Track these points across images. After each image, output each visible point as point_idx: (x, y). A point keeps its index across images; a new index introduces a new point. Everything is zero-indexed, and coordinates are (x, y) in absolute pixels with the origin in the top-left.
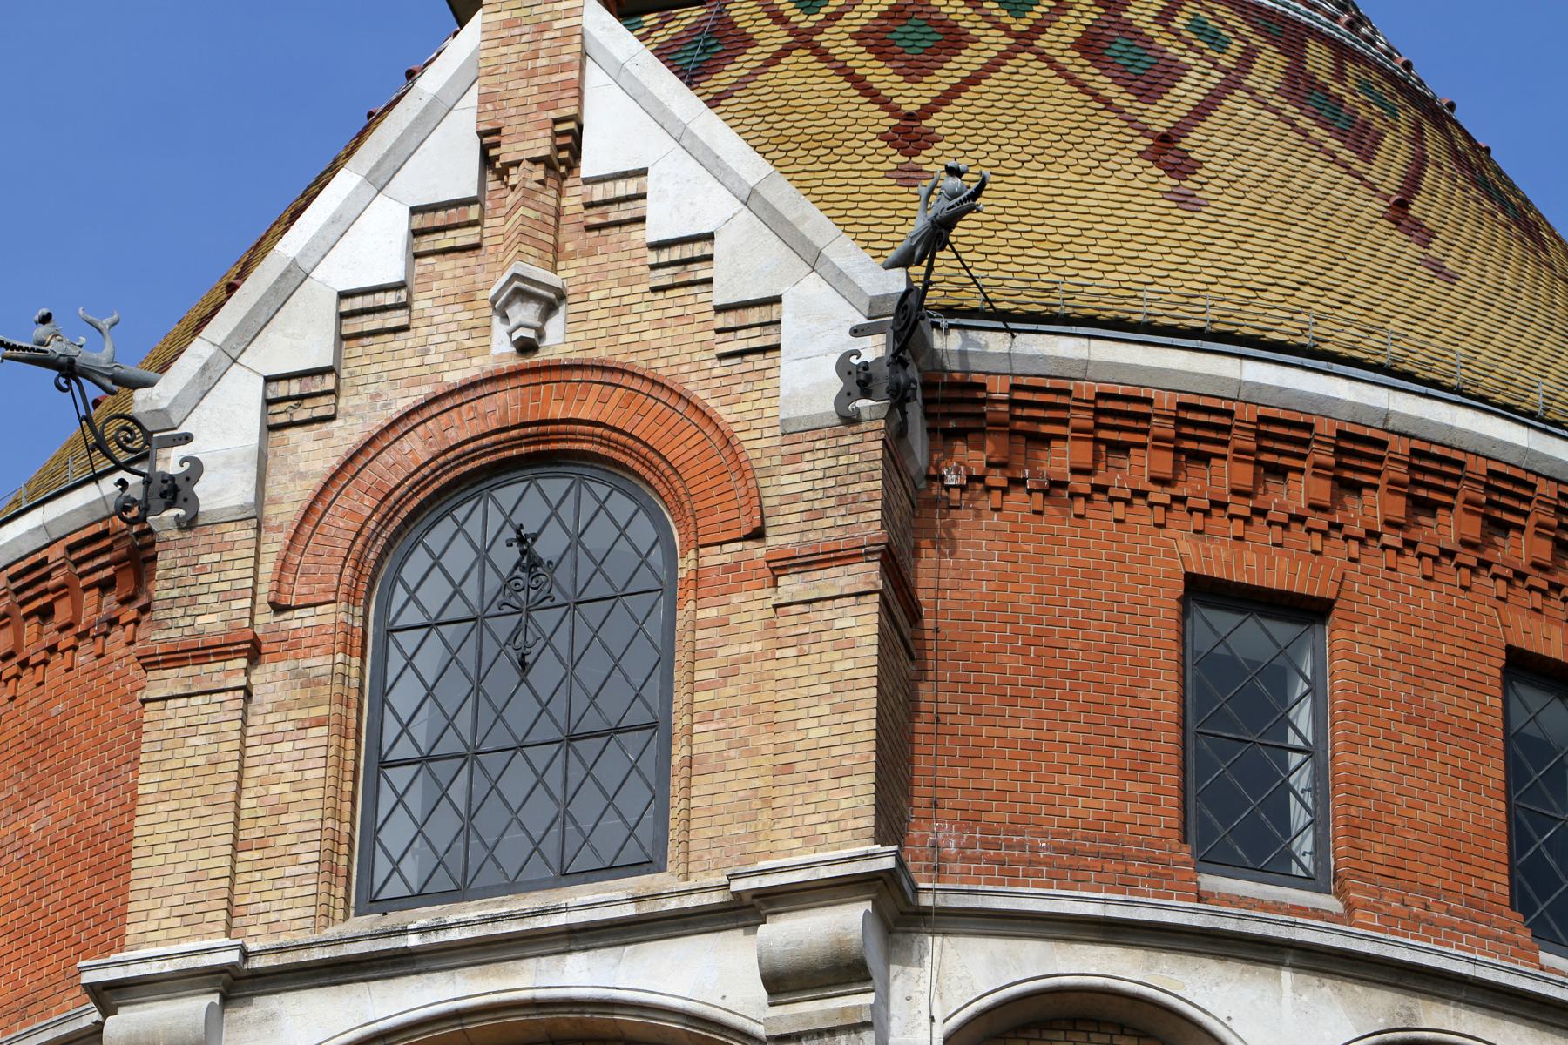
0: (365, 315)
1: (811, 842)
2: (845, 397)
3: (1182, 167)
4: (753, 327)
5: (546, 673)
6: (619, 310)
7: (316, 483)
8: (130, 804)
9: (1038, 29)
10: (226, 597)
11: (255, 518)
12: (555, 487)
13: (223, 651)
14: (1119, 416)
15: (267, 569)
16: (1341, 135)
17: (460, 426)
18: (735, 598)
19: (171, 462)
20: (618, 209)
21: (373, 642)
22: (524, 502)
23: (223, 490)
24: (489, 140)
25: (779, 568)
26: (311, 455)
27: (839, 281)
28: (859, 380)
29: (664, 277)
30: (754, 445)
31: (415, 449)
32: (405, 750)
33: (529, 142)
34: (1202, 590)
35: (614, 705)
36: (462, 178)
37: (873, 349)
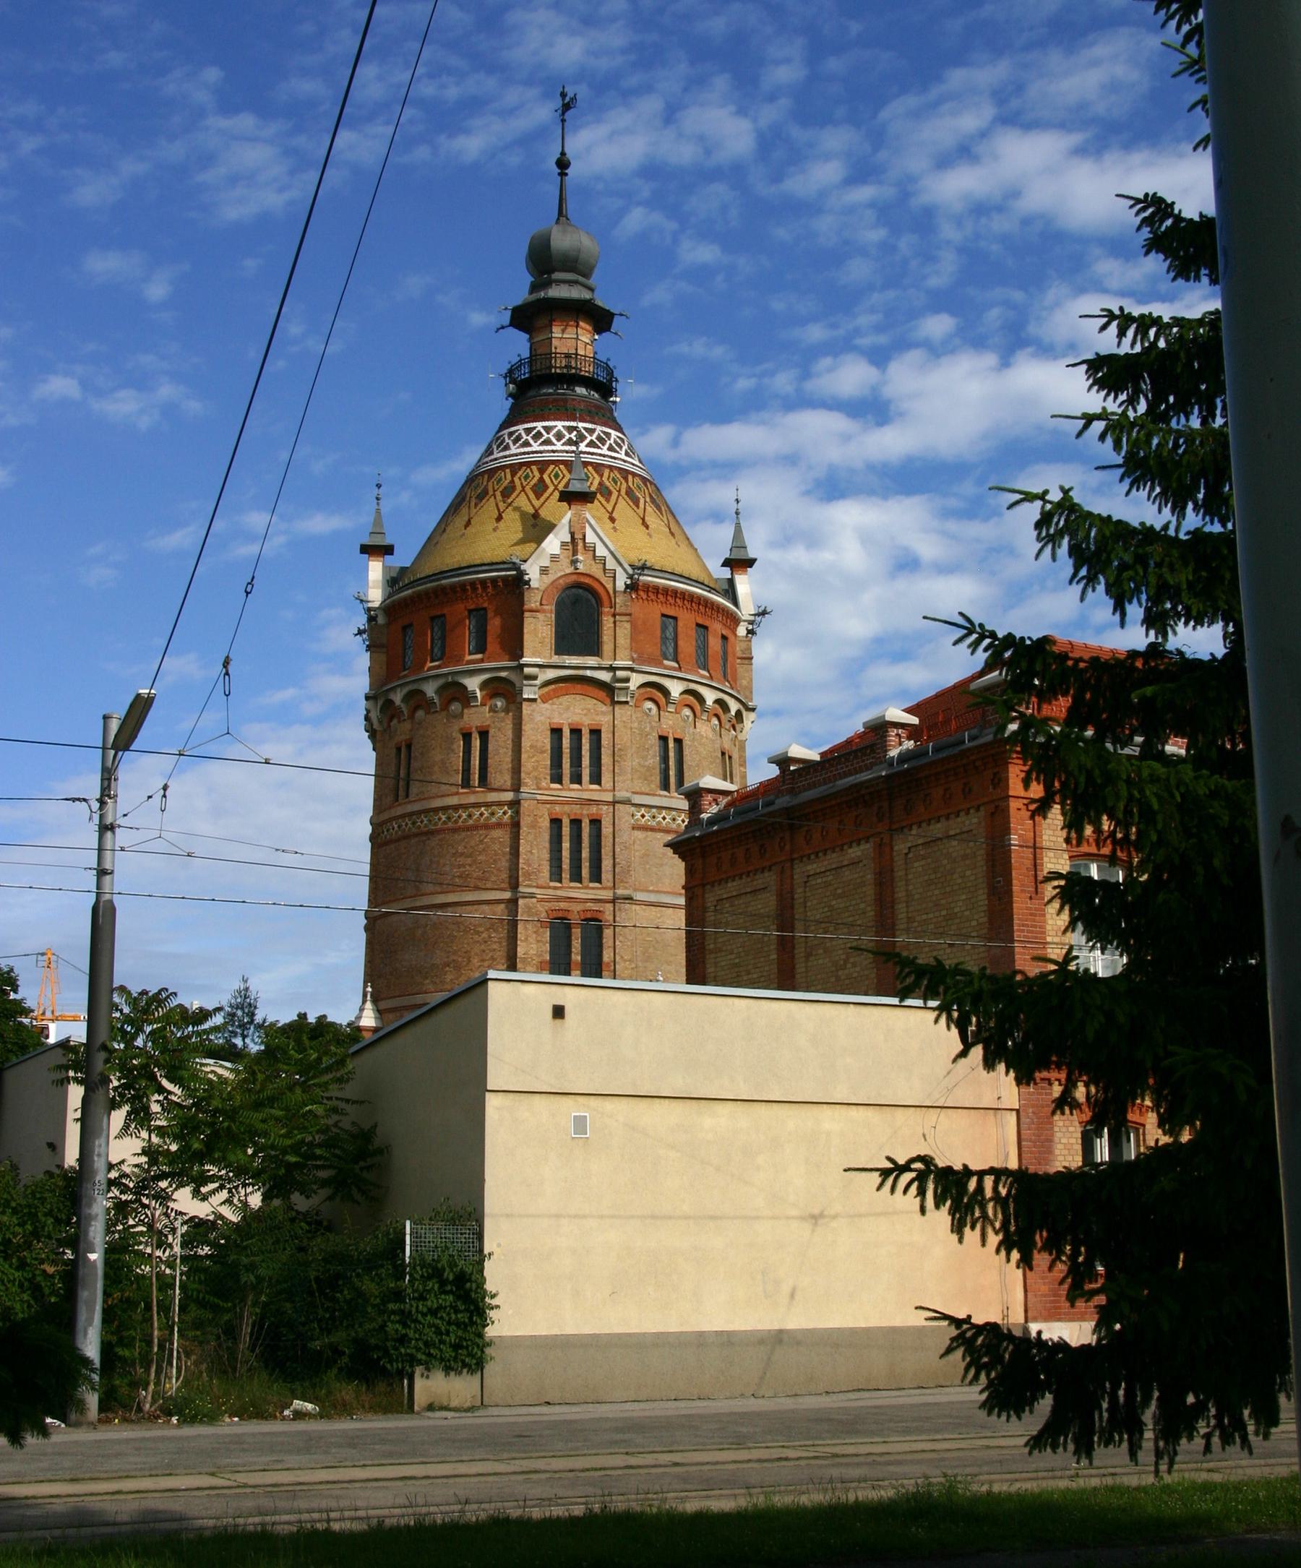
0: (554, 558)
14: (657, 590)
19: (526, 578)
23: (534, 584)
26: (548, 580)
27: (625, 570)
37: (629, 582)
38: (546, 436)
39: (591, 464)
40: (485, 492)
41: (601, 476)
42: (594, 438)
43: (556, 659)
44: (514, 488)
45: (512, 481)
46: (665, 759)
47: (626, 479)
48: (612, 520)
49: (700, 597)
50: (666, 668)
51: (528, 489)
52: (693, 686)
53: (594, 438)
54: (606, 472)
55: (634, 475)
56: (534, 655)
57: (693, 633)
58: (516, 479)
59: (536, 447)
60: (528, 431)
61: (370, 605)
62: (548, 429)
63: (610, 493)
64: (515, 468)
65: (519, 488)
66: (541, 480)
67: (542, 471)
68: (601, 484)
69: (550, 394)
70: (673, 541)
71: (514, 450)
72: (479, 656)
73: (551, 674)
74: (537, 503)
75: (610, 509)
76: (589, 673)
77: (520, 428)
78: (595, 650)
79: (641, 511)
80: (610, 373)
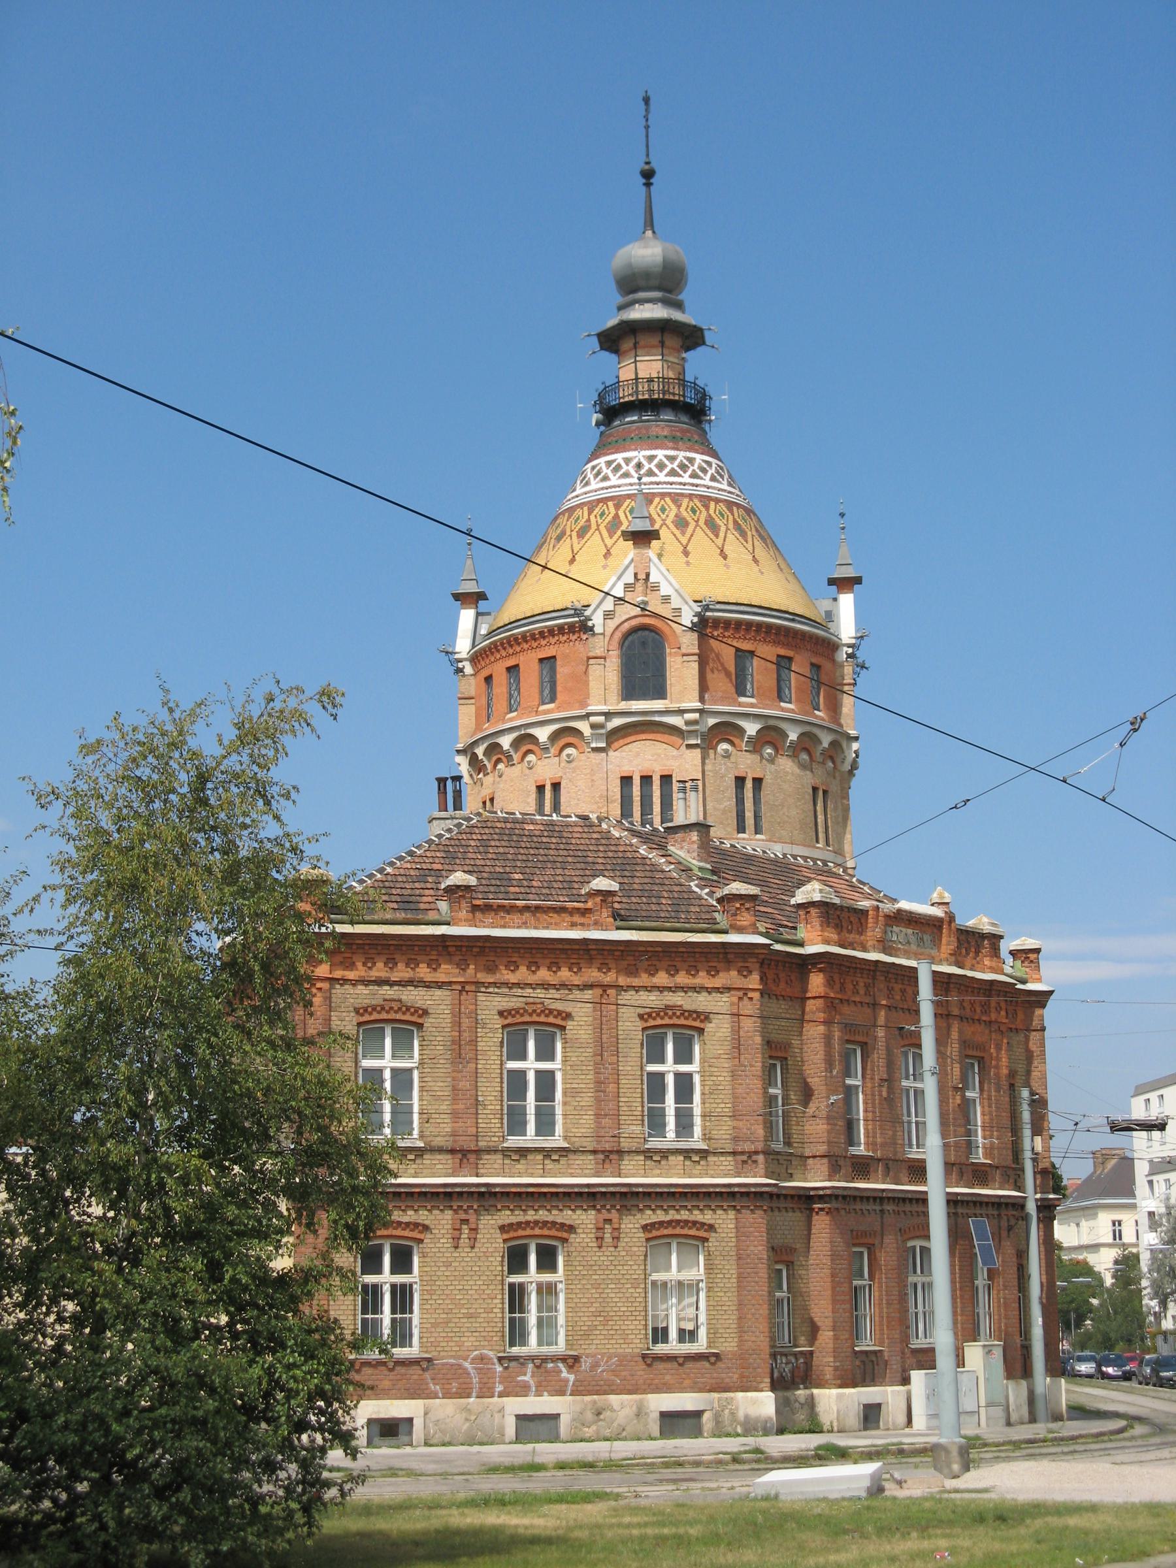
1: (690, 701)
11: (603, 634)
17: (634, 622)
19: (590, 624)
20: (656, 588)
24: (636, 574)
25: (684, 655)
26: (612, 624)
31: (627, 626)
33: (642, 576)
37: (696, 620)
38: (625, 468)
39: (670, 494)
40: (563, 533)
41: (679, 506)
42: (675, 465)
43: (624, 706)
44: (589, 526)
45: (589, 520)
46: (740, 801)
47: (707, 508)
48: (686, 553)
49: (779, 628)
50: (740, 705)
51: (602, 528)
52: (772, 722)
53: (675, 465)
54: (685, 502)
55: (717, 501)
56: (599, 703)
58: (592, 517)
59: (614, 480)
60: (609, 463)
61: (457, 656)
62: (627, 461)
63: (687, 524)
64: (592, 506)
65: (594, 526)
66: (617, 516)
67: (617, 507)
68: (676, 516)
69: (634, 422)
70: (756, 569)
71: (594, 485)
72: (552, 706)
73: (617, 722)
74: (609, 542)
75: (684, 542)
76: (657, 719)
77: (601, 461)
78: (661, 694)
79: (719, 542)
80: (703, 396)
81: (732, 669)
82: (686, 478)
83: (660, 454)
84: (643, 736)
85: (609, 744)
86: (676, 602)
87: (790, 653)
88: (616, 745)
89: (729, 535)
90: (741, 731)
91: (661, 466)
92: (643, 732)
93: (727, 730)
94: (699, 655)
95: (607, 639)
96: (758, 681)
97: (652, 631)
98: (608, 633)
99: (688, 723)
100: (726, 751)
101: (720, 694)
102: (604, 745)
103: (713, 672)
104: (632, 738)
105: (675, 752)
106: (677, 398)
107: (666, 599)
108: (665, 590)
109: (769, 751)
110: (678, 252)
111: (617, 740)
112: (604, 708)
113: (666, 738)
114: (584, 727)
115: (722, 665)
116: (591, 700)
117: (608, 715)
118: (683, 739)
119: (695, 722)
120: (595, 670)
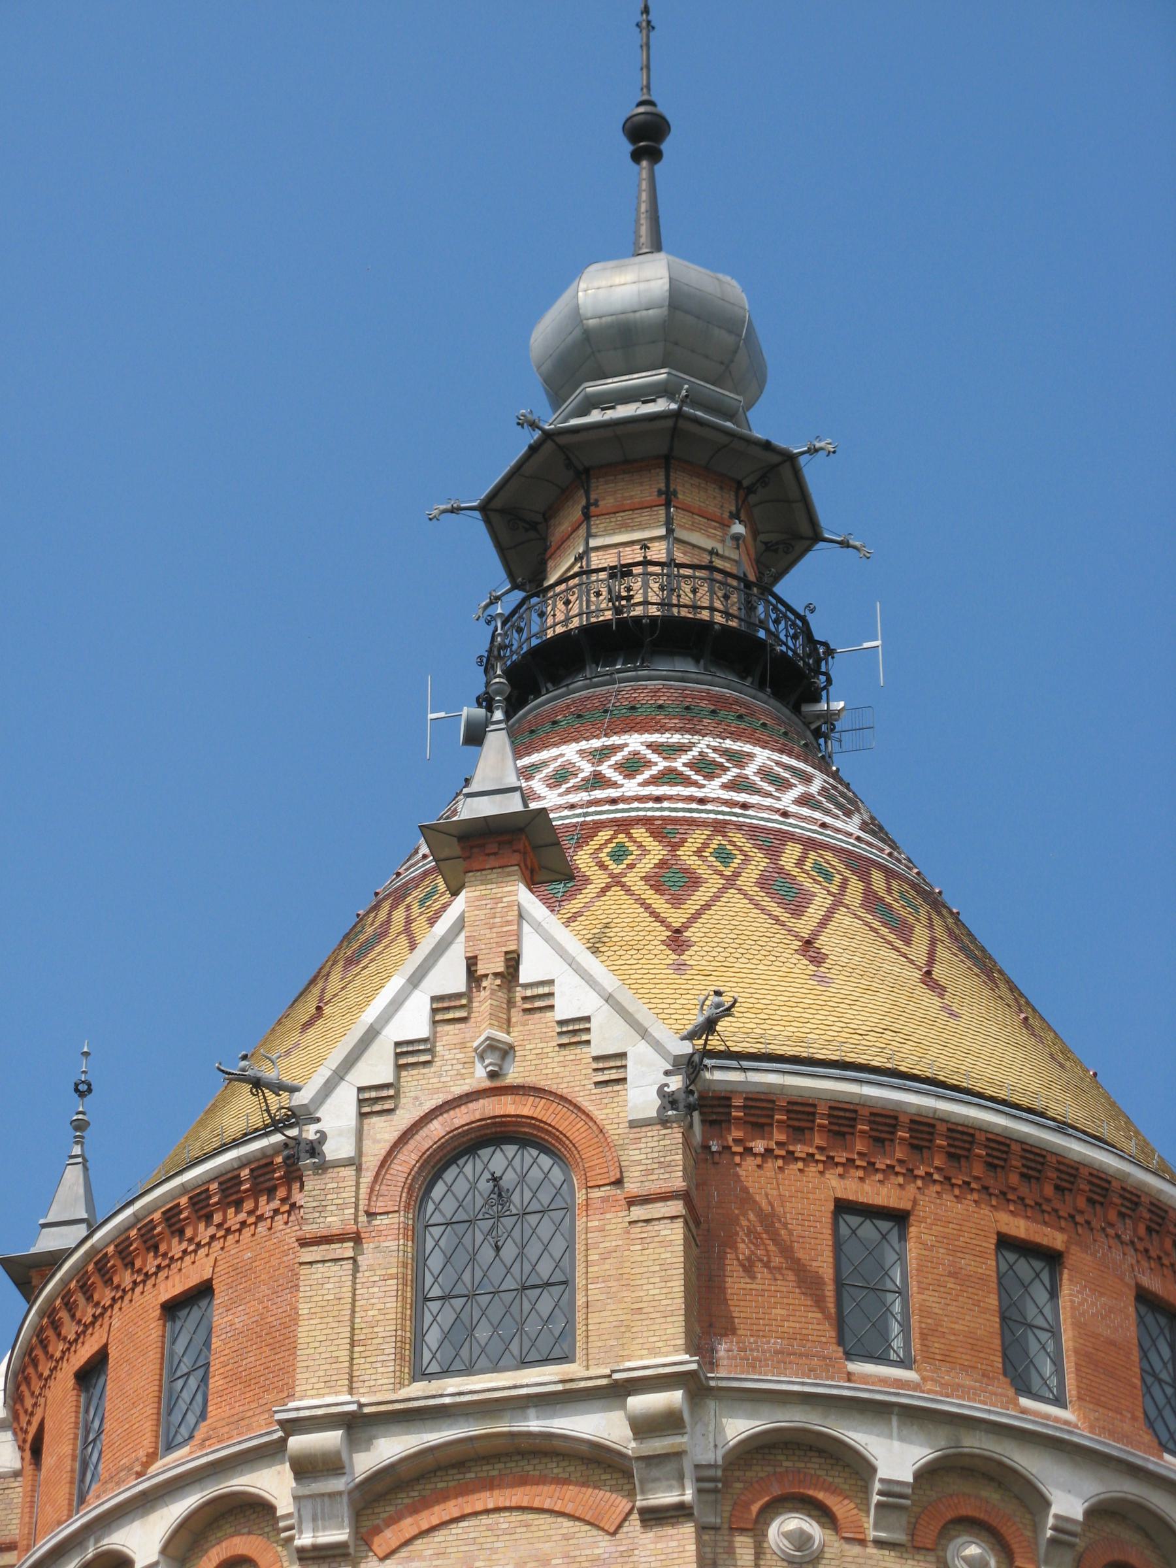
0: (410, 1055)
1: (653, 1352)
2: (662, 1108)
3: (818, 959)
4: (612, 1070)
5: (509, 1251)
6: (542, 1056)
7: (387, 1146)
8: (294, 1318)
9: (736, 874)
10: (342, 1207)
11: (355, 1163)
12: (510, 1150)
13: (340, 1238)
15: (364, 1191)
16: (893, 929)
18: (608, 1216)
19: (310, 1132)
20: (540, 1000)
21: (417, 1233)
22: (498, 1160)
23: (338, 1148)
25: (632, 1202)
26: (384, 1131)
27: (657, 1046)
28: (669, 1100)
29: (565, 1040)
30: (616, 1131)
31: (437, 1129)
32: (436, 1292)
33: (492, 964)
34: (843, 1207)
35: (545, 1269)
36: (457, 982)
37: (676, 1083)
39: (646, 822)
47: (773, 853)
52: (975, 1443)
53: (678, 764)
56: (330, 1385)
57: (988, 1267)
63: (693, 881)
68: (662, 864)
73: (389, 1448)
76: (534, 1424)
81: (824, 1265)
82: (713, 788)
83: (635, 742)
84: (488, 1499)
85: (364, 1537)
86: (607, 1035)
87: (1055, 1239)
88: (389, 1537)
89: (842, 918)
90: (857, 1468)
91: (632, 766)
92: (489, 1485)
93: (798, 1466)
94: (685, 1196)
95: (367, 1178)
96: (925, 1312)
97: (524, 1141)
98: (371, 1161)
99: (643, 1427)
100: (801, 1540)
101: (776, 1343)
102: (338, 1535)
103: (748, 1268)
104: (452, 1508)
105: (603, 1545)
106: (705, 615)
107: (575, 1031)
108: (571, 1001)
109: (973, 1550)
110: (726, 287)
111: (392, 1521)
112: (341, 1400)
113: (570, 1497)
114: (275, 1484)
115: (786, 1251)
116: (305, 1379)
117: (357, 1425)
118: (631, 1494)
119: (669, 1422)
120: (323, 1283)
